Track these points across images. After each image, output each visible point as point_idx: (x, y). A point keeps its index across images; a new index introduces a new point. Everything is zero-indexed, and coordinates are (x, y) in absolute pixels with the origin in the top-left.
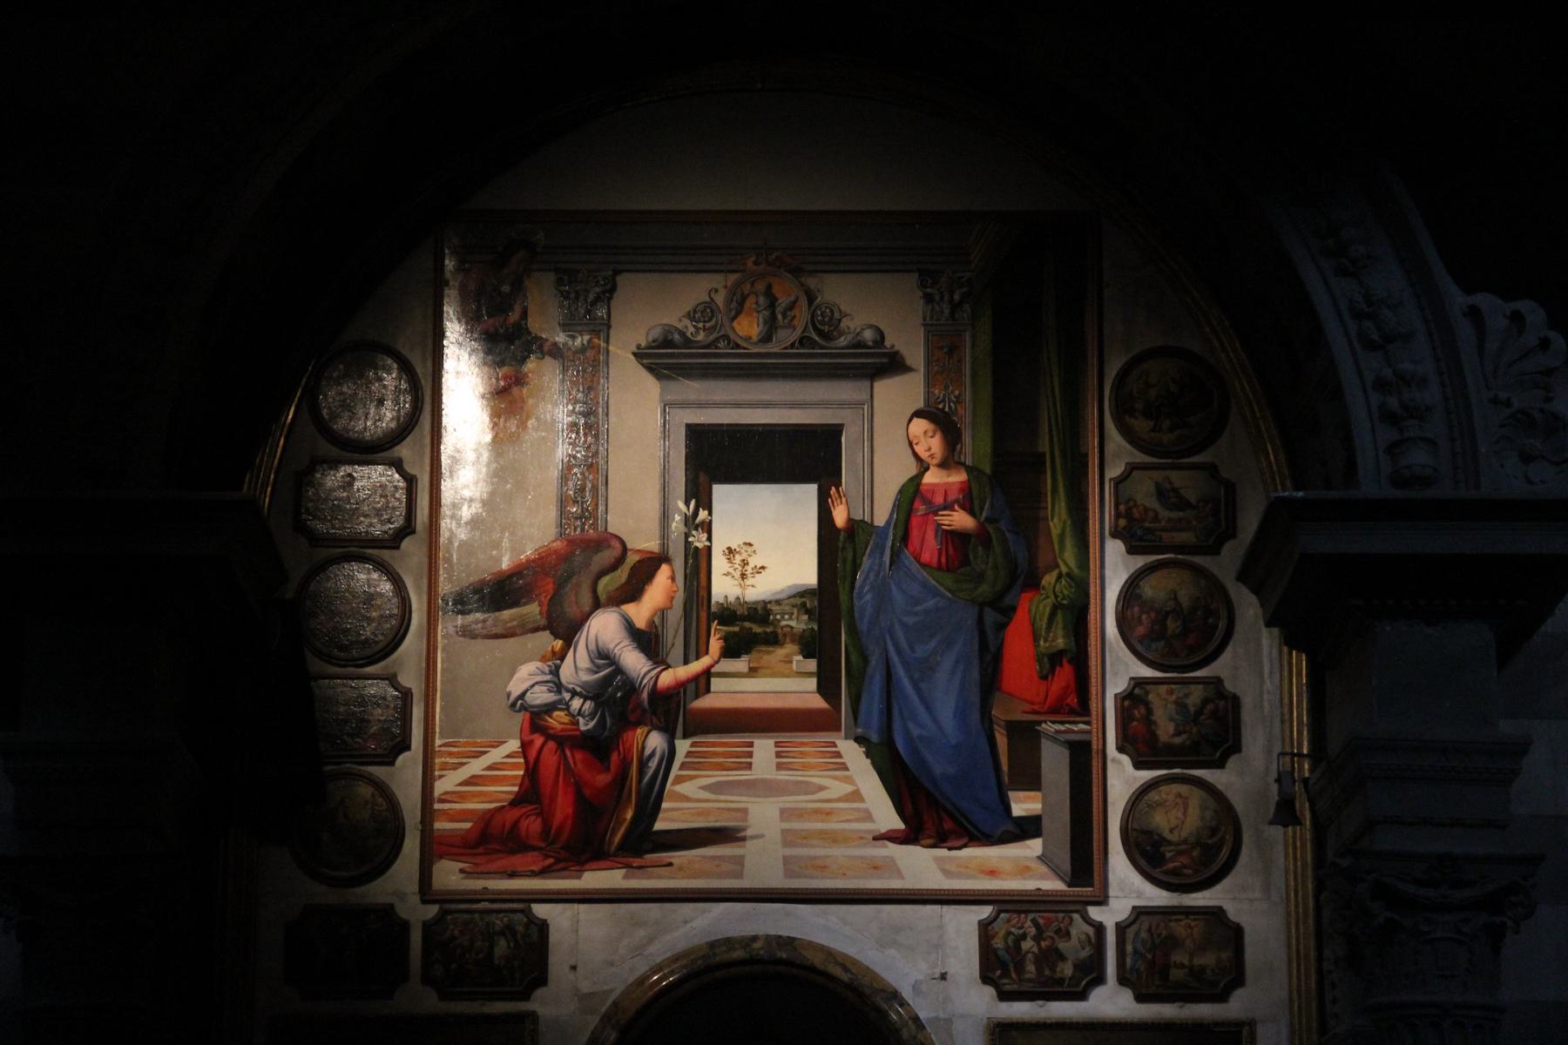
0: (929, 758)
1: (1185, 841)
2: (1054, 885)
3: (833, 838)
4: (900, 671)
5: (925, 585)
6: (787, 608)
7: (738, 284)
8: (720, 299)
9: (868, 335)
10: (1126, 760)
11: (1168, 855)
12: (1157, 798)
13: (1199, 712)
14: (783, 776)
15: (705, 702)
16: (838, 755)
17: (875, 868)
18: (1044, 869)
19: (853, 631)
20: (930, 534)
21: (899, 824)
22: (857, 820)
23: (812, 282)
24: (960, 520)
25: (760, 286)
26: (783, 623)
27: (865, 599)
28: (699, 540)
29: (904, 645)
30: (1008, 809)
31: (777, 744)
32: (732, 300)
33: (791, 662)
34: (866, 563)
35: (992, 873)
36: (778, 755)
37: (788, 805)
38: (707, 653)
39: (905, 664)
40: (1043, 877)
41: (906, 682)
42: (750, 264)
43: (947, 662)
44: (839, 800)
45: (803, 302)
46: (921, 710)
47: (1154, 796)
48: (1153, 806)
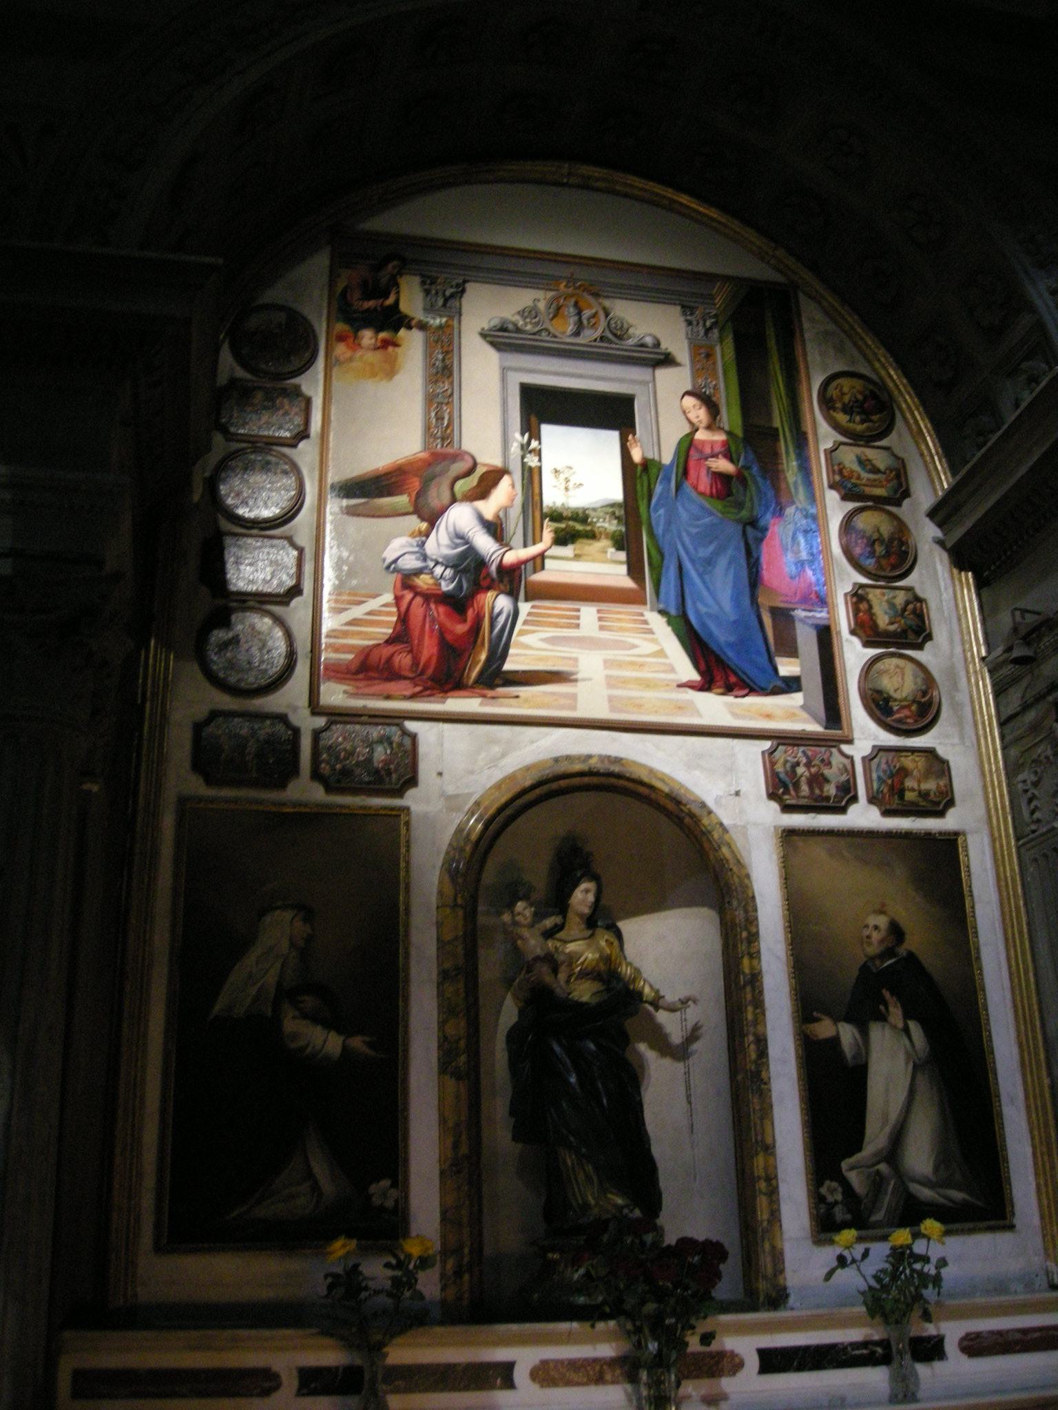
0: (713, 627)
1: (905, 699)
2: (814, 727)
3: (647, 684)
4: (688, 565)
5: (702, 507)
6: (601, 514)
7: (556, 299)
8: (542, 306)
9: (649, 340)
10: (856, 641)
11: (895, 708)
12: (882, 667)
13: (904, 610)
14: (605, 635)
15: (539, 577)
16: (646, 622)
17: (680, 707)
18: (805, 715)
19: (651, 534)
20: (703, 473)
21: (695, 676)
22: (664, 672)
23: (607, 303)
24: (723, 465)
25: (572, 301)
26: (598, 525)
27: (659, 516)
28: (532, 461)
29: (690, 547)
30: (776, 670)
31: (599, 611)
32: (550, 308)
33: (606, 552)
34: (658, 489)
35: (769, 716)
36: (600, 619)
37: (609, 657)
38: (541, 540)
39: (693, 561)
40: (805, 721)
41: (693, 574)
42: (562, 286)
43: (722, 562)
44: (648, 656)
45: (602, 315)
46: (705, 593)
47: (880, 666)
48: (881, 673)
